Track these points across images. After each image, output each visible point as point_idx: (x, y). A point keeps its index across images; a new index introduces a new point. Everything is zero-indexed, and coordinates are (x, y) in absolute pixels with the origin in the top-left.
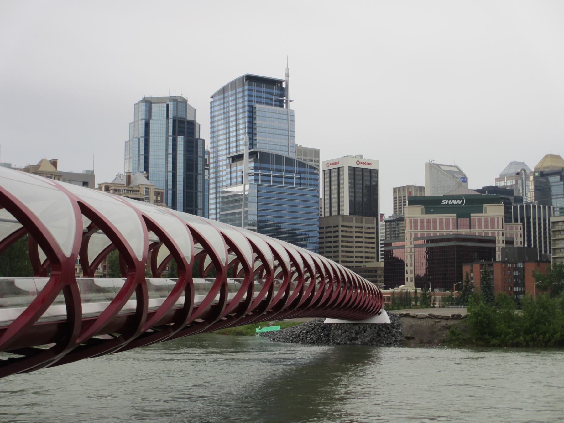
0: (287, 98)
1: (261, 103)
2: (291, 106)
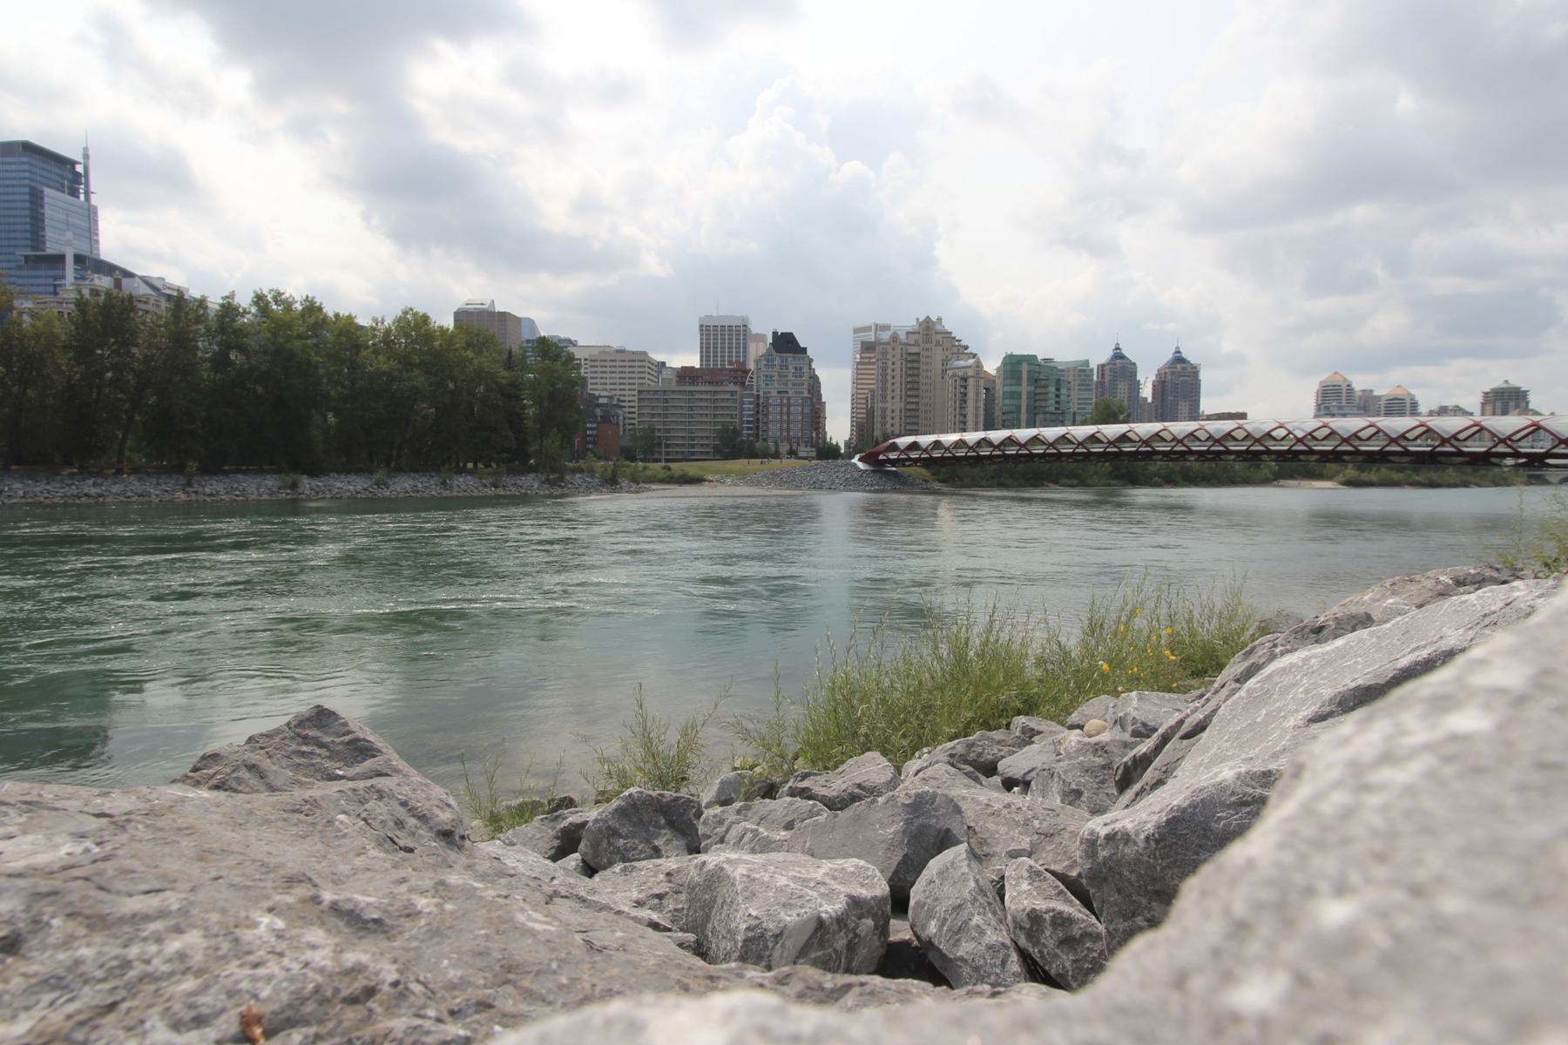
0: (87, 185)
1: (48, 186)
2: (94, 200)
